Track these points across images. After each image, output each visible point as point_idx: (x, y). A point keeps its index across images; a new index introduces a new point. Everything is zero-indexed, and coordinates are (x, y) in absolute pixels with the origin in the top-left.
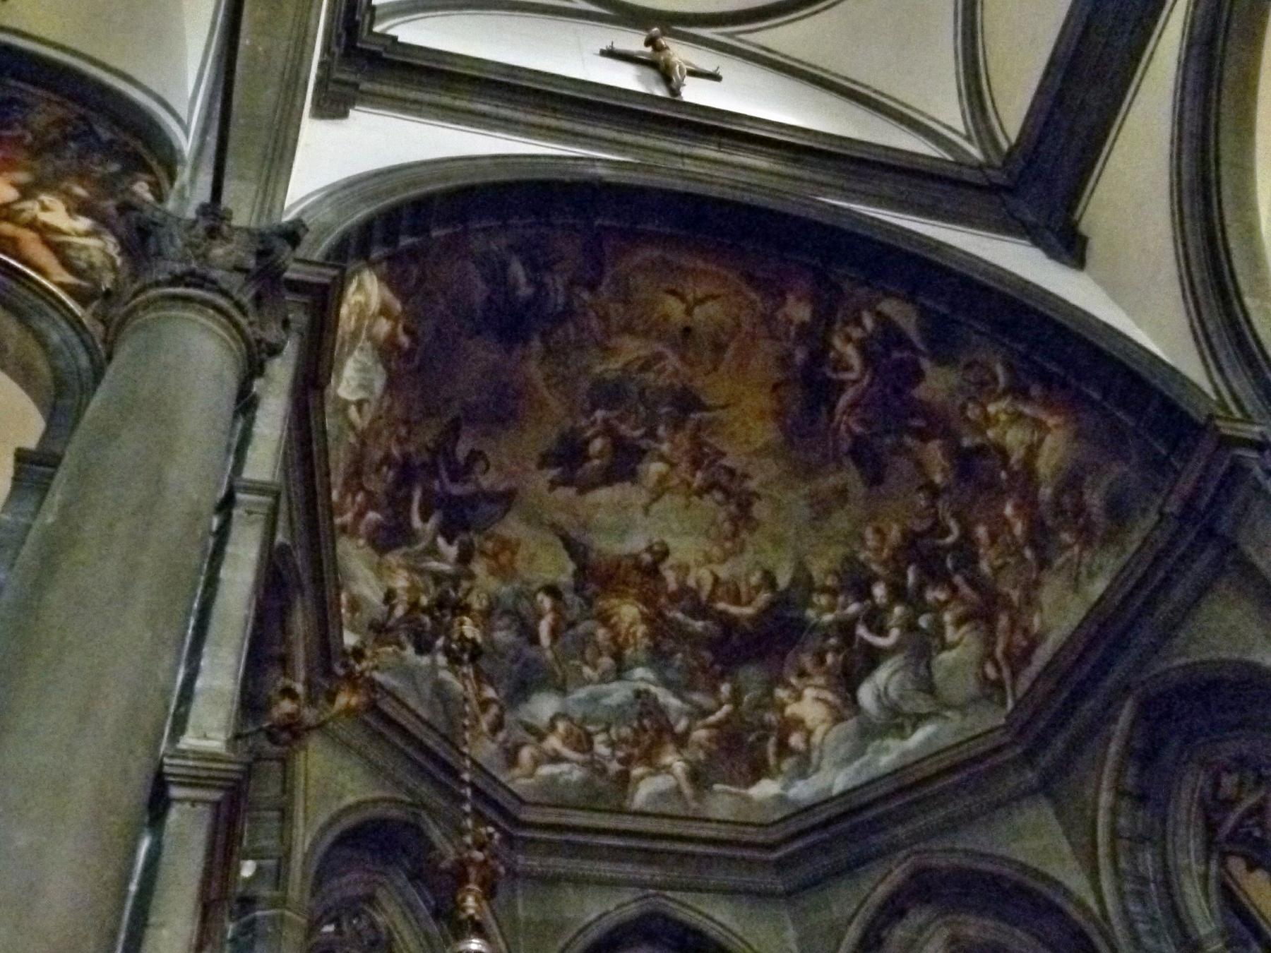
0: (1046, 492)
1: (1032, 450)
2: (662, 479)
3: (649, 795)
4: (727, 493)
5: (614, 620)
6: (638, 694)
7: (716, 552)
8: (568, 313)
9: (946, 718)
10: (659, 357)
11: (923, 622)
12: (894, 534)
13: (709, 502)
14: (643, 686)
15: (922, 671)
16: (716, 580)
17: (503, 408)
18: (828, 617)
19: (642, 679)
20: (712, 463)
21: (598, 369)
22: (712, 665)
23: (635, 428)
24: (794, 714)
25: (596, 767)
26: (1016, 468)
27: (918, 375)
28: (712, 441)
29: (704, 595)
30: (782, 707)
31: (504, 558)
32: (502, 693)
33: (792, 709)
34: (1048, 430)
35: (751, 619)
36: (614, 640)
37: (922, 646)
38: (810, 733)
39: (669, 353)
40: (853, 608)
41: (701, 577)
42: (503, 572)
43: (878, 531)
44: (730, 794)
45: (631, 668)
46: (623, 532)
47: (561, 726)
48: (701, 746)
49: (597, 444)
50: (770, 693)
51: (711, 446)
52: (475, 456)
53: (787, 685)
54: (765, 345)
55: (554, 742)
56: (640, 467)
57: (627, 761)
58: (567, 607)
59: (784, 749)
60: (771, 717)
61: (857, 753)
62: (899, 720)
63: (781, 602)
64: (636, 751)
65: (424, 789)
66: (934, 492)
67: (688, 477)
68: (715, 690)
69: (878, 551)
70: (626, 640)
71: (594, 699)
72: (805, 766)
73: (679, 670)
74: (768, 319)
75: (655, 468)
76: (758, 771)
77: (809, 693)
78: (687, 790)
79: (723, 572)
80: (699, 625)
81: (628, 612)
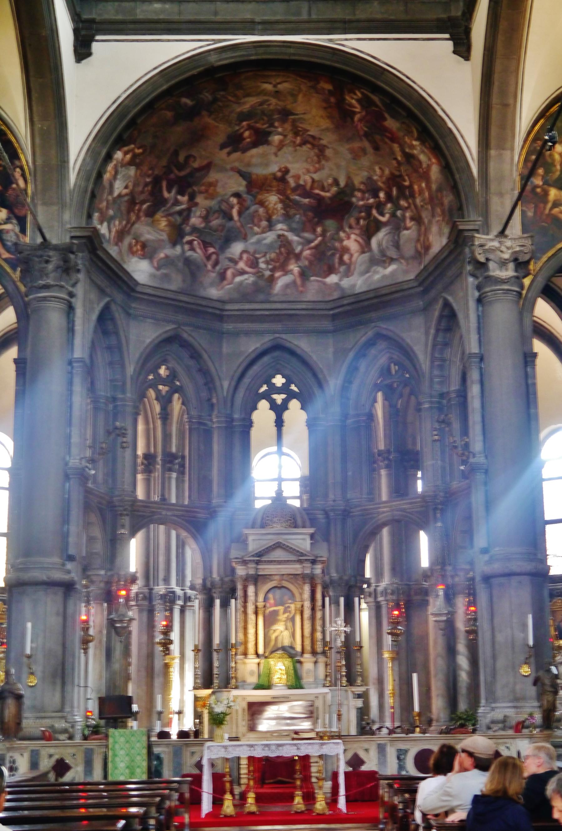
0: (434, 187)
1: (429, 167)
2: (281, 141)
3: (282, 286)
4: (314, 146)
5: (267, 203)
6: (279, 236)
7: (312, 168)
8: (215, 100)
9: (401, 263)
10: (267, 101)
11: (399, 213)
12: (387, 172)
13: (305, 148)
14: (281, 232)
15: (396, 238)
16: (313, 181)
17: (198, 137)
18: (361, 203)
19: (281, 229)
20: (303, 134)
21: (239, 110)
22: (314, 218)
23: (263, 124)
24: (346, 245)
25: (259, 275)
26: (425, 170)
27: (385, 119)
28: (301, 125)
29: (308, 187)
30: (341, 241)
31: (211, 190)
32: (217, 246)
33: (346, 243)
34: (433, 163)
35: (330, 198)
36: (267, 212)
37: (397, 226)
38: (352, 255)
39: (271, 99)
40: (371, 201)
41: (306, 179)
42: (211, 197)
43: (380, 168)
44: (317, 281)
45: (275, 224)
46: (267, 165)
47: (245, 256)
48: (306, 258)
49: (247, 134)
50: (337, 233)
51: (302, 128)
52: (188, 158)
53: (344, 231)
54: (315, 95)
55: (241, 265)
56: (270, 139)
57: (273, 270)
58: (244, 201)
59: (341, 262)
60: (337, 244)
61: (367, 271)
62: (384, 259)
63: (341, 193)
64: (278, 264)
65: (180, 318)
66: (399, 163)
67: (294, 140)
68: (314, 231)
69: (381, 176)
70: (273, 212)
71: (259, 242)
72: (348, 273)
73: (298, 222)
74: (313, 87)
75: (276, 138)
76: (331, 270)
77: (353, 237)
78: (299, 281)
79: (316, 176)
80: (306, 201)
81: (273, 199)
